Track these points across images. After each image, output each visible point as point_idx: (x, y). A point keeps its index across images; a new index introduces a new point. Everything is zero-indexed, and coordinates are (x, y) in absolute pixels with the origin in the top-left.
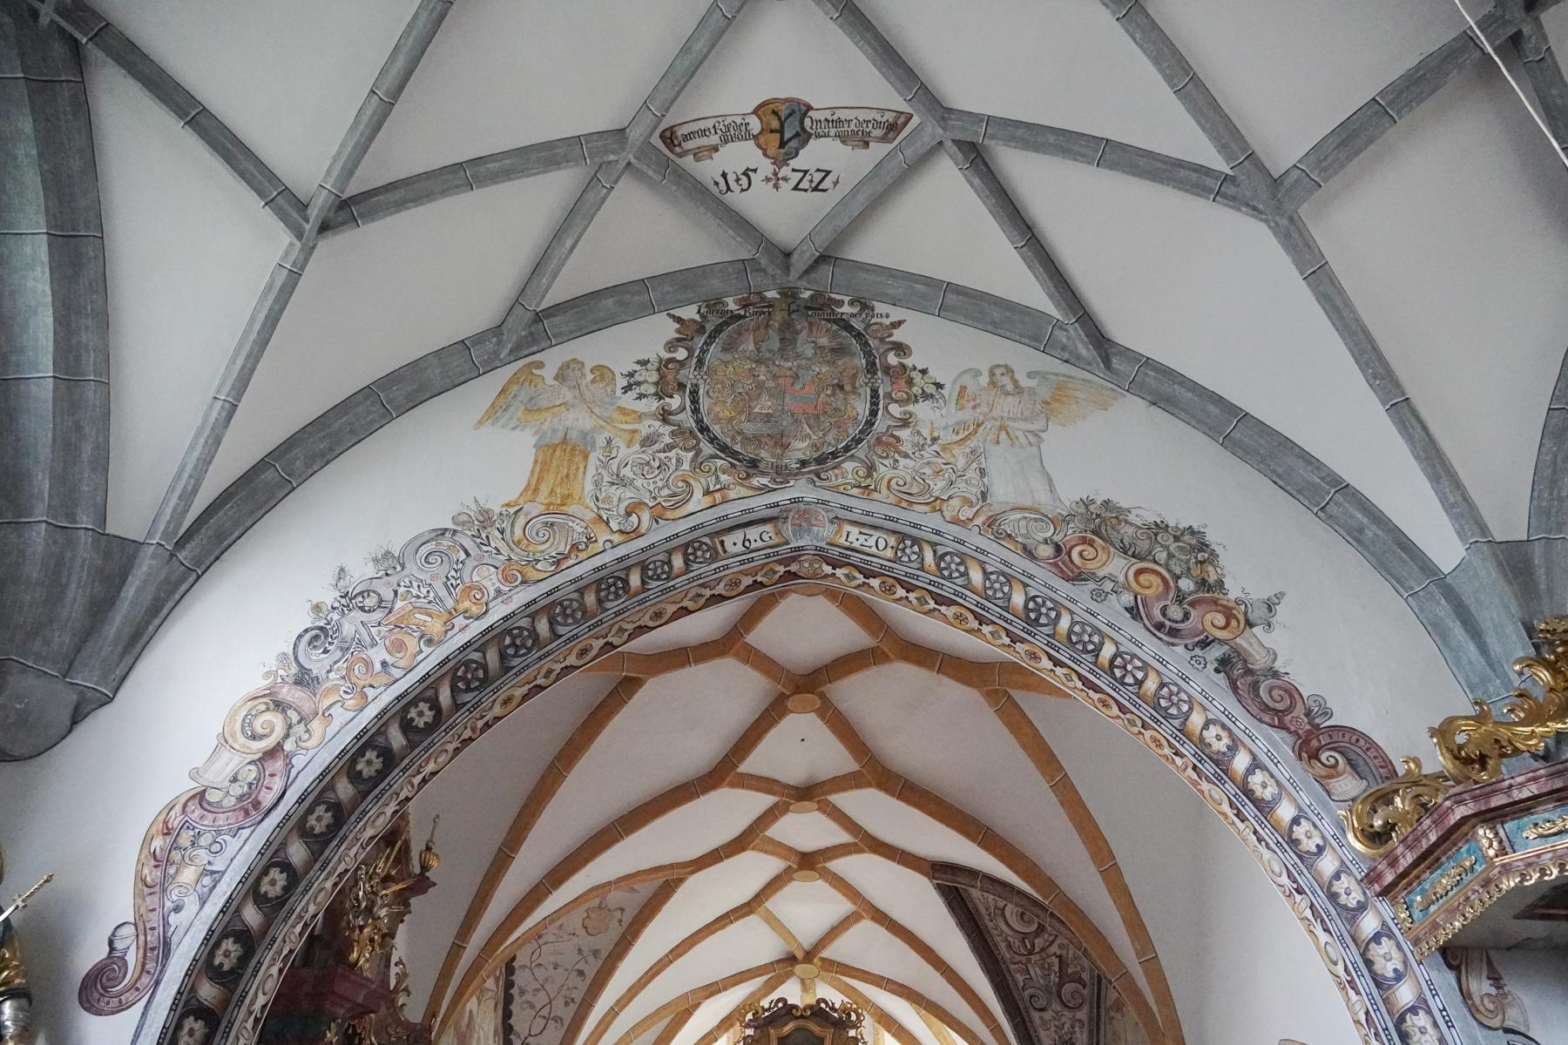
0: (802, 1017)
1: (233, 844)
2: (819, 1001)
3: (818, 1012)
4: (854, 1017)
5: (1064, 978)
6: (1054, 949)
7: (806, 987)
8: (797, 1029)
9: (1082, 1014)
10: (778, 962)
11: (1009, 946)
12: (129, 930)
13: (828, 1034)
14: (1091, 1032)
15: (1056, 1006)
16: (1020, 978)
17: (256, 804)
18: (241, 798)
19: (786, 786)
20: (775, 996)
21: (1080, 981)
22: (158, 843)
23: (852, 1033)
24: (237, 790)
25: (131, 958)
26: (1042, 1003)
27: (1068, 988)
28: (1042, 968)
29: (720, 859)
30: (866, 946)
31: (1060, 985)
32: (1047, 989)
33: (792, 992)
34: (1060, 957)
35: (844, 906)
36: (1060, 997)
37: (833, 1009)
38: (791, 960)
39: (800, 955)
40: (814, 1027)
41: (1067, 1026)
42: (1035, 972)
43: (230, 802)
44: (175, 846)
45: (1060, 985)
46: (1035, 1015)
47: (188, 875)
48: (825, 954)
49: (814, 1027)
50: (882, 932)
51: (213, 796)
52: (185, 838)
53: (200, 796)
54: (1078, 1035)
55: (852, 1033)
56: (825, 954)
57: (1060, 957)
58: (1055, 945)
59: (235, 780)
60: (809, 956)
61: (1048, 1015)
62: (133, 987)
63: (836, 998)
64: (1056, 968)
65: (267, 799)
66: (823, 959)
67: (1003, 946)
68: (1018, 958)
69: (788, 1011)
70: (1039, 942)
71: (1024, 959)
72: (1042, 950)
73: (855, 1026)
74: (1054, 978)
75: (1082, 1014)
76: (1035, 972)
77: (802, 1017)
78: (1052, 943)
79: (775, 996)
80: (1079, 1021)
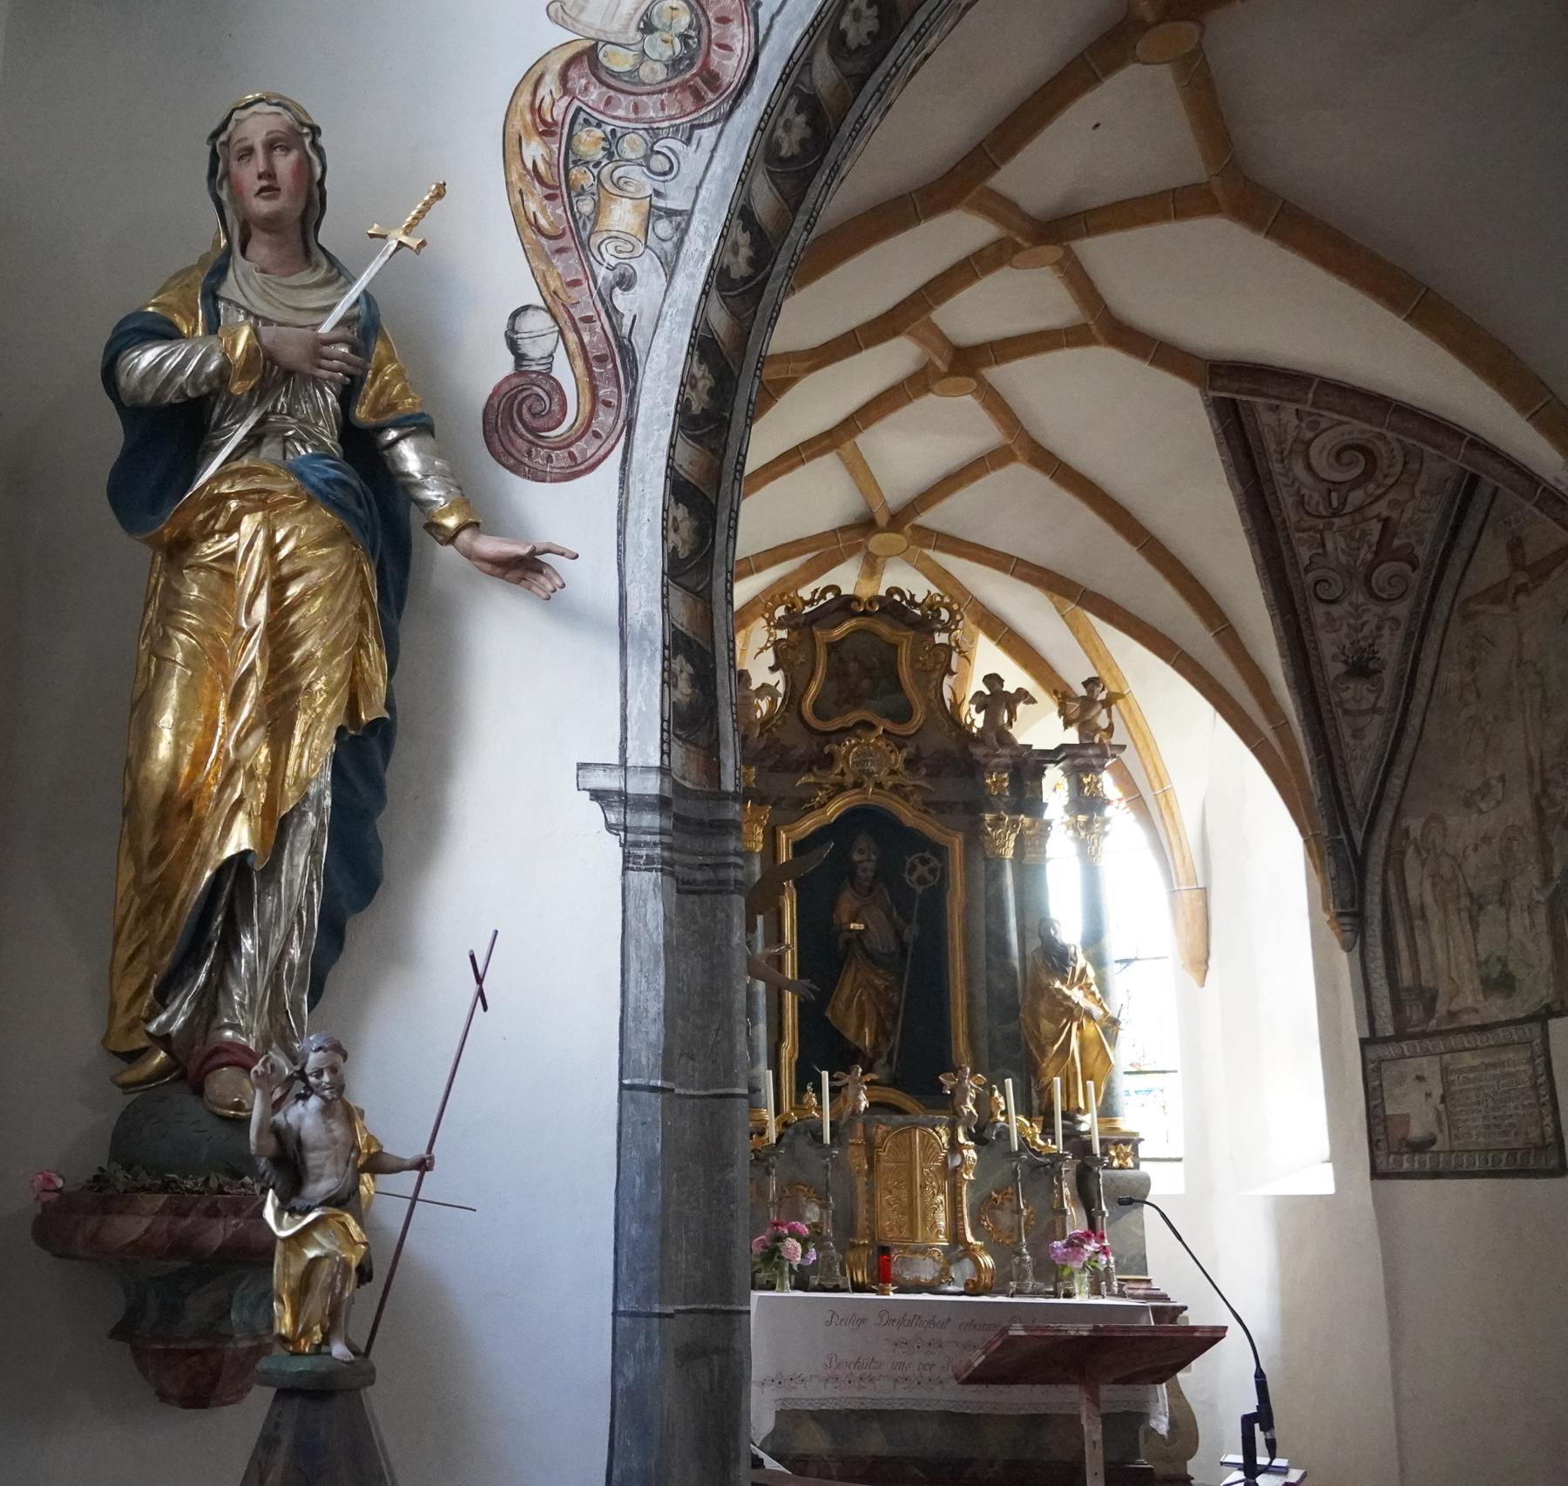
0: (865, 613)
1: (691, 159)
2: (890, 592)
3: (893, 607)
4: (945, 615)
5: (1383, 550)
6: (1381, 508)
7: (872, 567)
8: (856, 631)
9: (1401, 610)
10: (844, 529)
11: (1301, 501)
12: (537, 322)
13: (905, 641)
14: (1409, 636)
15: (1359, 597)
16: (1305, 554)
17: (712, 79)
18: (674, 65)
19: (1025, 216)
20: (821, 583)
22: (534, 150)
23: (940, 638)
24: (662, 49)
25: (563, 371)
27: (1386, 569)
29: (857, 349)
30: (1014, 507)
31: (1372, 566)
33: (847, 577)
34: (1386, 522)
35: (988, 435)
37: (912, 602)
38: (866, 525)
39: (882, 520)
40: (884, 629)
41: (1371, 626)
42: (1335, 544)
43: (654, 72)
44: (571, 158)
45: (1372, 566)
46: (1318, 611)
47: (622, 216)
48: (925, 519)
49: (884, 629)
50: (1039, 481)
51: (618, 61)
52: (589, 142)
53: (588, 57)
55: (940, 638)
56: (925, 519)
57: (1386, 522)
59: (648, 28)
60: (899, 519)
61: (1336, 610)
62: (586, 428)
63: (918, 587)
64: (1375, 538)
65: (730, 68)
66: (920, 528)
67: (1288, 501)
69: (844, 605)
70: (1357, 497)
71: (1320, 524)
72: (1359, 509)
73: (946, 629)
74: (1366, 555)
75: (1401, 610)
76: (1335, 544)
77: (865, 613)
78: (1378, 498)
79: (821, 583)
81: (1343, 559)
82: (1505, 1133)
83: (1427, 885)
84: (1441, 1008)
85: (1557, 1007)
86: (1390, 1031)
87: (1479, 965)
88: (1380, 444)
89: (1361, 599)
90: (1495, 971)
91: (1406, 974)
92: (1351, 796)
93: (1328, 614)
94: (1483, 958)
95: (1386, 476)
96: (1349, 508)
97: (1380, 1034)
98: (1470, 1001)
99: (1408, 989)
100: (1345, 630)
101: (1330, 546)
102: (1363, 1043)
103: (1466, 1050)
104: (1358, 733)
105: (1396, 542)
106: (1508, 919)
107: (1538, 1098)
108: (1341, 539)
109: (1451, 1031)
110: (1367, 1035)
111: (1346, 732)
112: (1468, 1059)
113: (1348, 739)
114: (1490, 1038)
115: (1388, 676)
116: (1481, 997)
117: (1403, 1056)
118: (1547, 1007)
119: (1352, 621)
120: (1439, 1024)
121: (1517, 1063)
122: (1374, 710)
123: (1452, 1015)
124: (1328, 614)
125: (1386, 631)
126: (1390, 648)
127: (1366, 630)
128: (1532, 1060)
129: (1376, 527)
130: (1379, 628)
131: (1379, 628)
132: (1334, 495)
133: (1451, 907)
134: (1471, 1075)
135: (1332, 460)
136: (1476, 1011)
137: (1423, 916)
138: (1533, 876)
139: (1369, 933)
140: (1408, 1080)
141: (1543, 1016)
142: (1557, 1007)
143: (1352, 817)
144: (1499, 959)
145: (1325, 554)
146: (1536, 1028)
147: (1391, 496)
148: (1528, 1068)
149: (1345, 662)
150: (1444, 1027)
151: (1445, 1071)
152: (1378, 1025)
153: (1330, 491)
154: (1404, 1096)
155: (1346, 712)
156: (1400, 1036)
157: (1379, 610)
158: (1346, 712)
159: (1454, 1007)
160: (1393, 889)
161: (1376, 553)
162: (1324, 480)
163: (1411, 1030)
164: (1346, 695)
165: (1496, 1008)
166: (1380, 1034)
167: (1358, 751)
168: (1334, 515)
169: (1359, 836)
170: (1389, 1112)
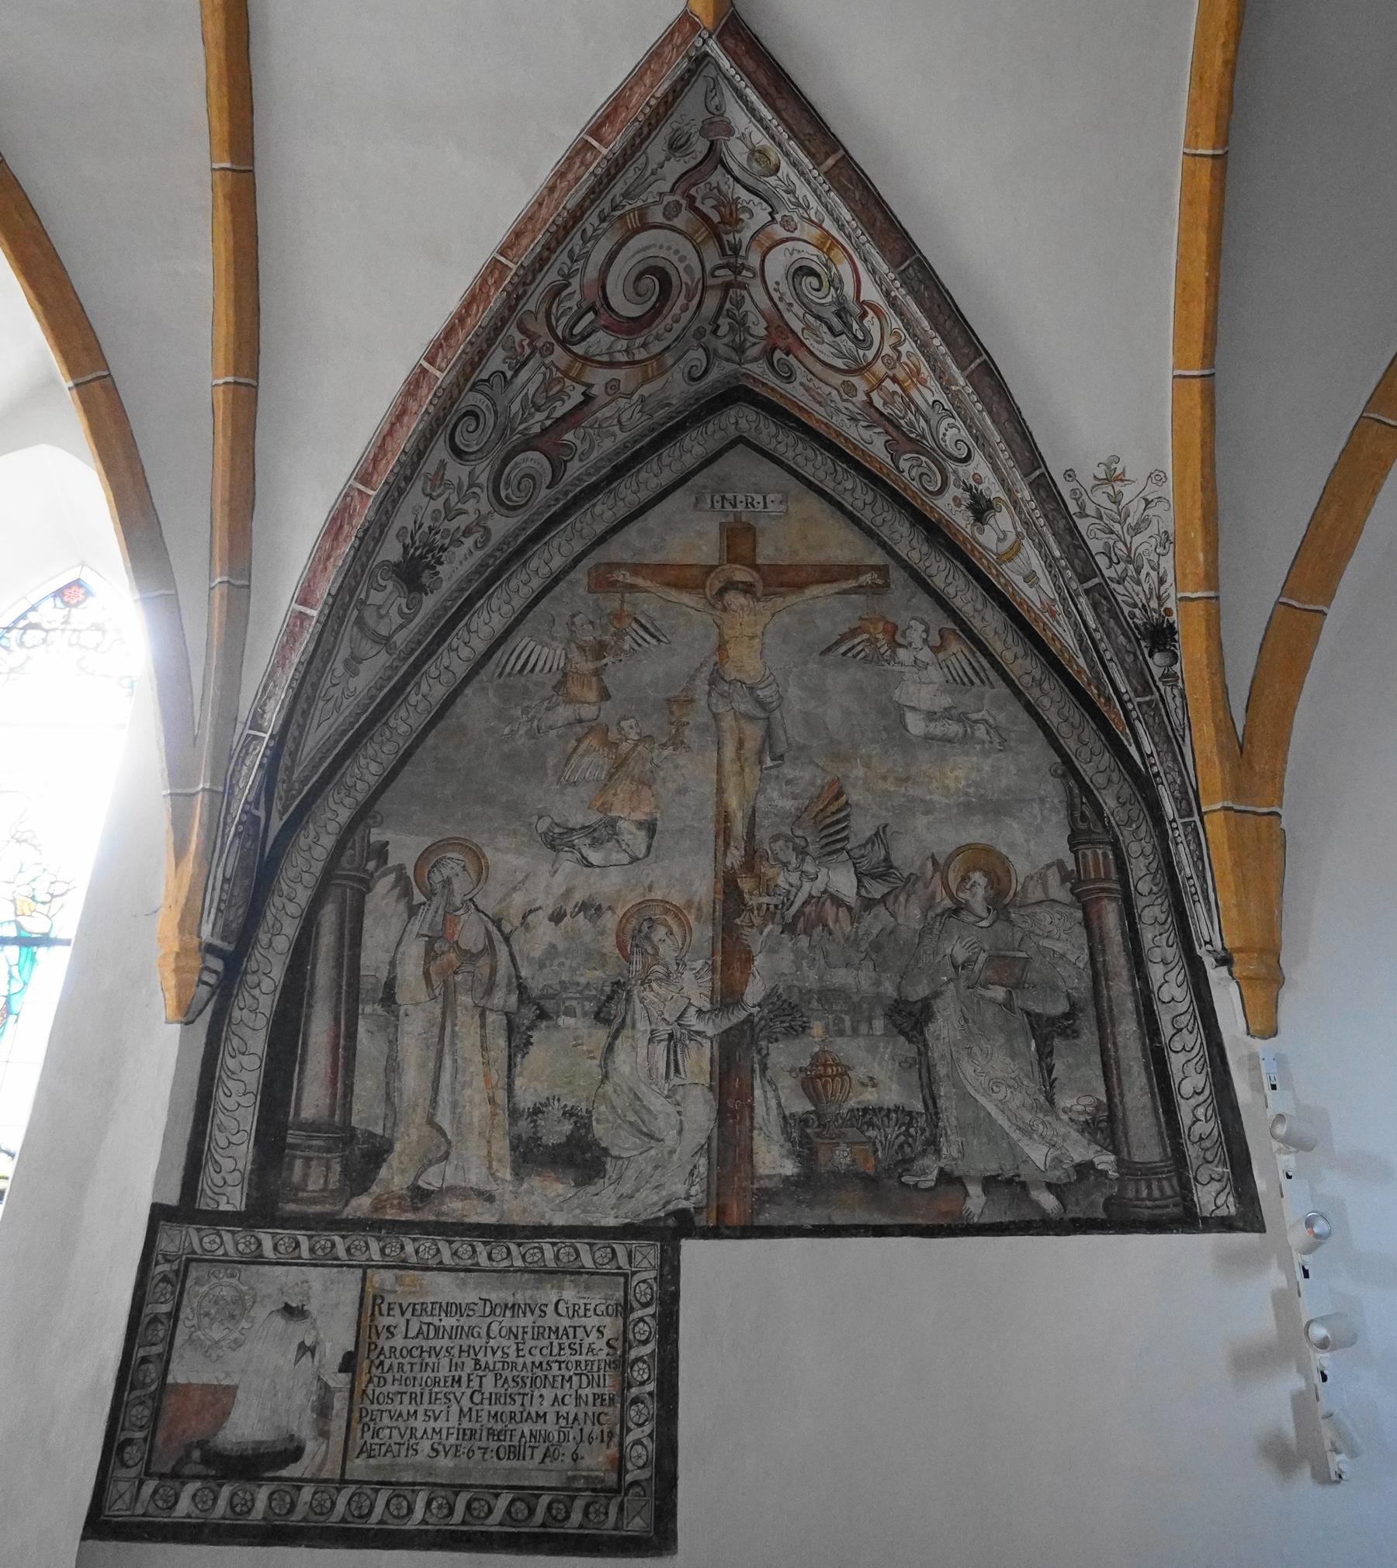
6: (599, 378)
9: (501, 526)
21: (558, 468)
26: (467, 439)
28: (547, 384)
32: (504, 430)
36: (505, 461)
41: (462, 522)
42: (530, 379)
54: (461, 551)
58: (608, 374)
61: (457, 472)
64: (561, 410)
68: (540, 328)
70: (602, 340)
71: (545, 336)
72: (586, 359)
74: (537, 422)
76: (530, 379)
78: (612, 364)
80: (487, 530)
81: (516, 407)
82: (515, 1453)
83: (414, 950)
84: (394, 1176)
85: (701, 1221)
86: (234, 1200)
87: (514, 1114)
88: (682, 300)
89: (483, 479)
90: (556, 1131)
91: (312, 1098)
92: (293, 755)
93: (443, 465)
94: (526, 1099)
95: (644, 345)
96: (579, 349)
97: (204, 1204)
98: (475, 1177)
99: (312, 1127)
100: (439, 504)
101: (524, 374)
102: (159, 1215)
103: (441, 1268)
104: (354, 662)
105: (569, 436)
106: (610, 1048)
107: (626, 1384)
108: (539, 377)
109: (407, 1227)
110: (172, 1198)
111: (344, 652)
112: (443, 1287)
113: (339, 667)
114: (517, 1254)
115: (429, 602)
116: (506, 1174)
117: (258, 1260)
118: (682, 1215)
119: (454, 498)
120: (377, 1207)
121: (585, 1314)
122: (386, 642)
123: (420, 1195)
124: (443, 465)
125: (469, 542)
126: (455, 568)
127: (453, 525)
128: (625, 1309)
129: (576, 397)
130: (467, 532)
131: (467, 532)
132: (591, 316)
133: (465, 999)
134: (449, 1322)
135: (661, 263)
136: (490, 1198)
137: (388, 996)
138: (694, 988)
139: (244, 999)
140: (260, 1313)
141: (673, 1230)
142: (701, 1221)
143: (280, 789)
144: (569, 1113)
145: (507, 382)
146: (648, 1255)
147: (619, 373)
148: (612, 1326)
149: (406, 548)
150: (390, 1215)
151: (369, 1305)
152: (210, 1178)
153: (592, 308)
154: (237, 1344)
155: (360, 622)
156: (262, 1211)
157: (485, 507)
158: (360, 622)
159: (431, 1179)
160: (326, 940)
161: (545, 431)
162: (603, 287)
163: (291, 1207)
164: (376, 597)
165: (548, 1199)
166: (204, 1204)
167: (336, 692)
168: (564, 343)
169: (276, 825)
170: (178, 1374)
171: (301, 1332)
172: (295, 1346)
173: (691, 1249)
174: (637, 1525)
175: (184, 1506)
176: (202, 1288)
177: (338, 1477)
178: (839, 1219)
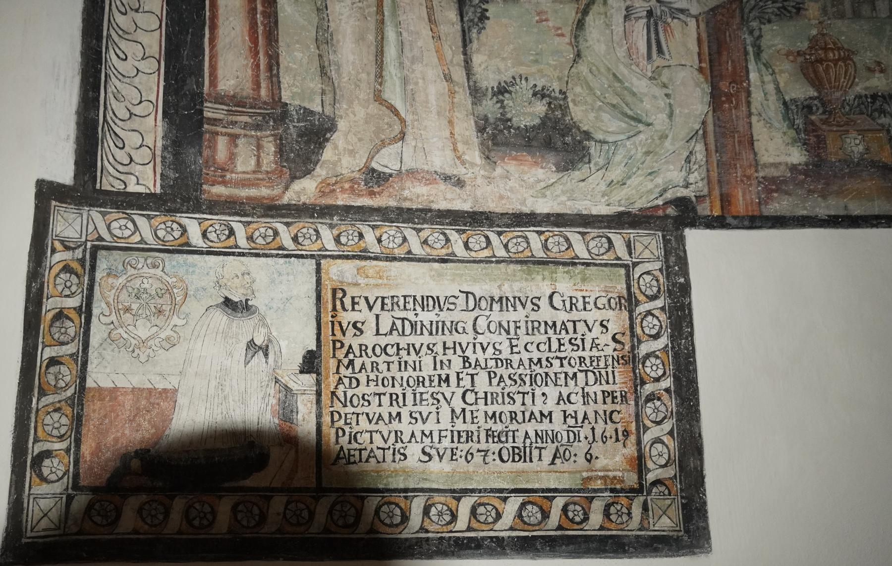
82: (520, 455)
84: (342, 156)
85: (704, 209)
86: (146, 179)
87: (476, 93)
90: (528, 113)
94: (488, 79)
97: (108, 183)
98: (440, 159)
99: (236, 102)
103: (410, 258)
106: (580, 25)
107: (639, 381)
109: (364, 213)
110: (64, 173)
112: (416, 280)
116: (474, 155)
117: (185, 249)
118: (681, 203)
120: (326, 189)
121: (585, 302)
123: (375, 178)
128: (629, 302)
134: (426, 317)
136: (460, 183)
140: (194, 308)
141: (682, 215)
142: (704, 209)
144: (540, 94)
146: (649, 245)
148: (617, 321)
150: (342, 200)
151: (328, 301)
152: (109, 155)
154: (170, 344)
156: (181, 192)
159: (387, 161)
163: (219, 190)
165: (527, 184)
166: (108, 183)
170: (99, 376)
171: (245, 329)
172: (243, 346)
173: (696, 239)
174: (665, 523)
175: (129, 521)
176: (112, 282)
177: (314, 485)
178: (856, 210)
